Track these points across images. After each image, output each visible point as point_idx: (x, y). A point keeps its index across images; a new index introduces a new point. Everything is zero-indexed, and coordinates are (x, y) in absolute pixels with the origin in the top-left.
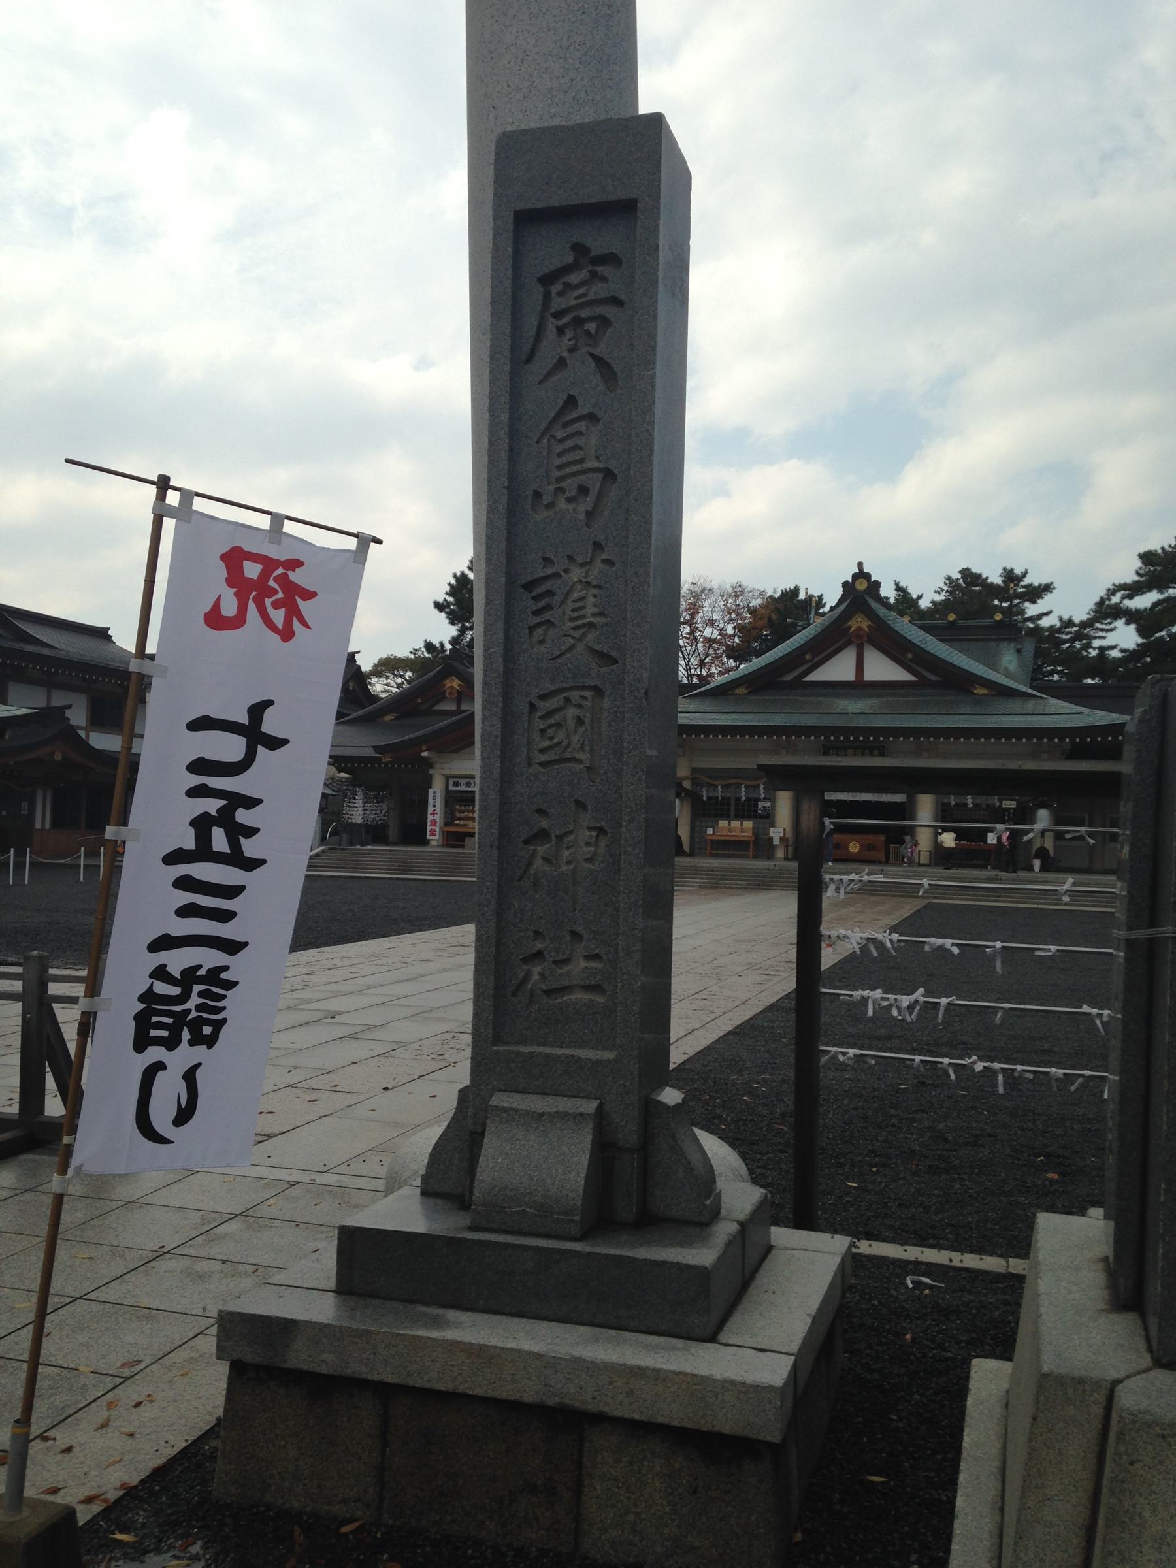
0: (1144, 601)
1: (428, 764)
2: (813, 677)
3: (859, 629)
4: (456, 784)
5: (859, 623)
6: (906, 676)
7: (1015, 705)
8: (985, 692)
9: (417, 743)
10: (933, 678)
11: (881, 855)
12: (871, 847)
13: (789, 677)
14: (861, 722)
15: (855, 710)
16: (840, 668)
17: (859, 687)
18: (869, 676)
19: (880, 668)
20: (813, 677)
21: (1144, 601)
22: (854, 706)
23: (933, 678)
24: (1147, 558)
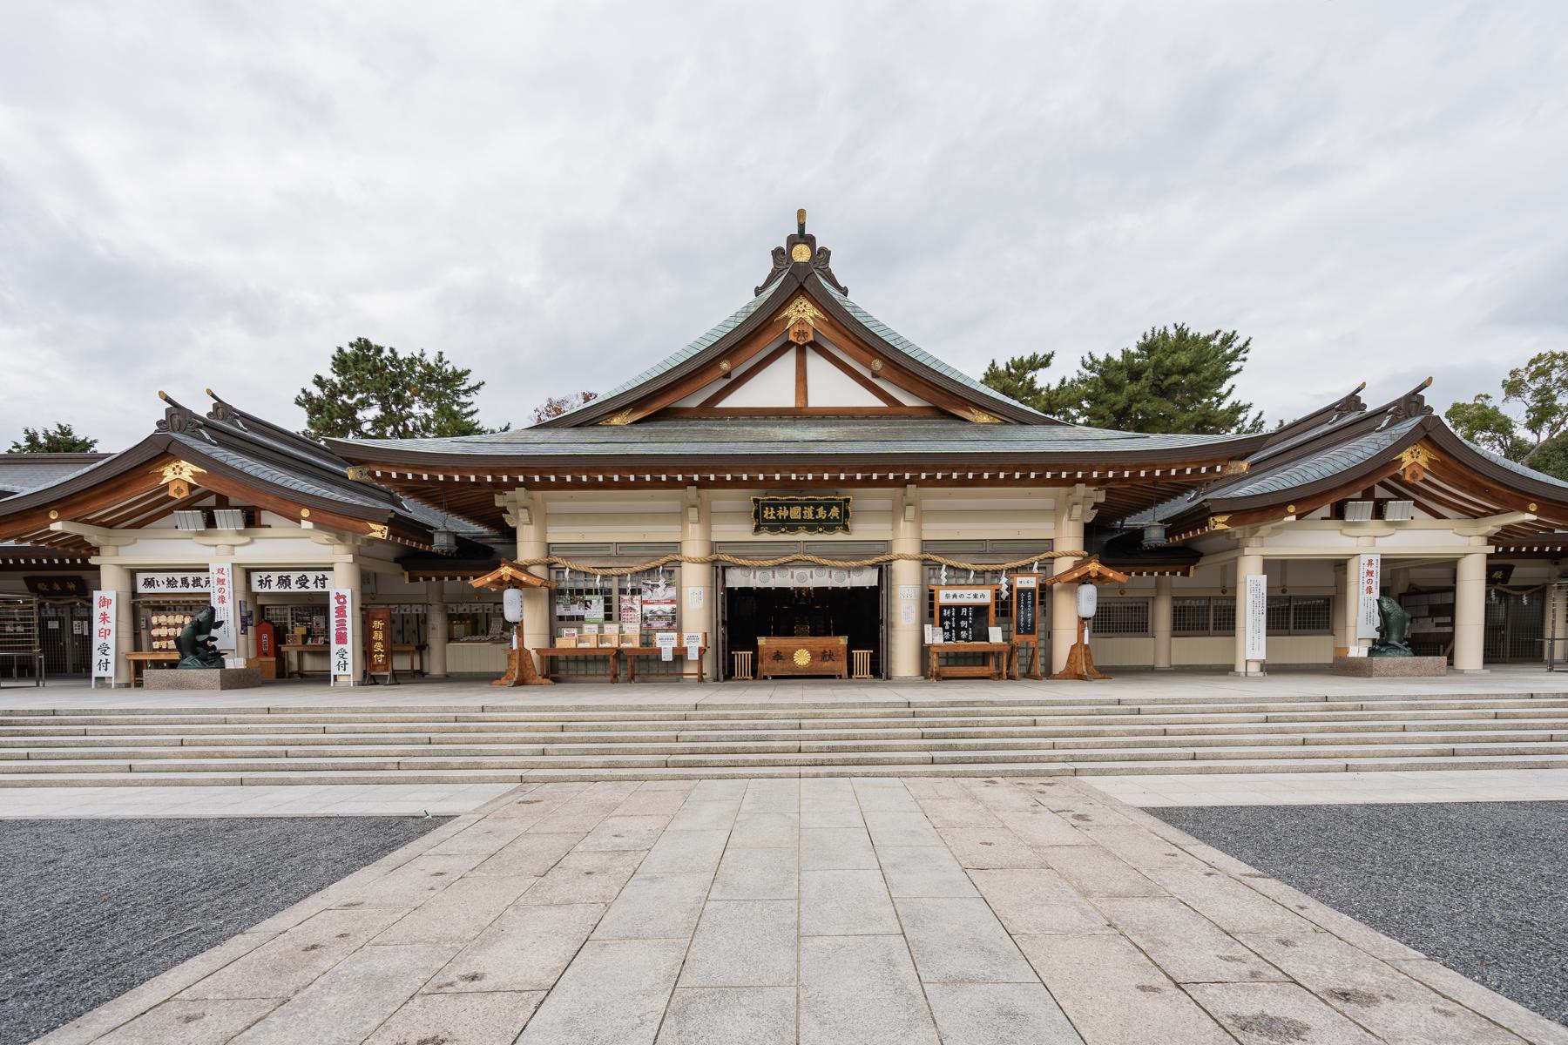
2: (728, 402)
3: (801, 322)
4: (149, 583)
5: (803, 312)
6: (871, 401)
8: (985, 419)
10: (908, 401)
11: (842, 667)
12: (826, 655)
13: (694, 402)
16: (772, 387)
17: (800, 414)
18: (816, 400)
19: (832, 387)
20: (728, 402)
23: (908, 401)
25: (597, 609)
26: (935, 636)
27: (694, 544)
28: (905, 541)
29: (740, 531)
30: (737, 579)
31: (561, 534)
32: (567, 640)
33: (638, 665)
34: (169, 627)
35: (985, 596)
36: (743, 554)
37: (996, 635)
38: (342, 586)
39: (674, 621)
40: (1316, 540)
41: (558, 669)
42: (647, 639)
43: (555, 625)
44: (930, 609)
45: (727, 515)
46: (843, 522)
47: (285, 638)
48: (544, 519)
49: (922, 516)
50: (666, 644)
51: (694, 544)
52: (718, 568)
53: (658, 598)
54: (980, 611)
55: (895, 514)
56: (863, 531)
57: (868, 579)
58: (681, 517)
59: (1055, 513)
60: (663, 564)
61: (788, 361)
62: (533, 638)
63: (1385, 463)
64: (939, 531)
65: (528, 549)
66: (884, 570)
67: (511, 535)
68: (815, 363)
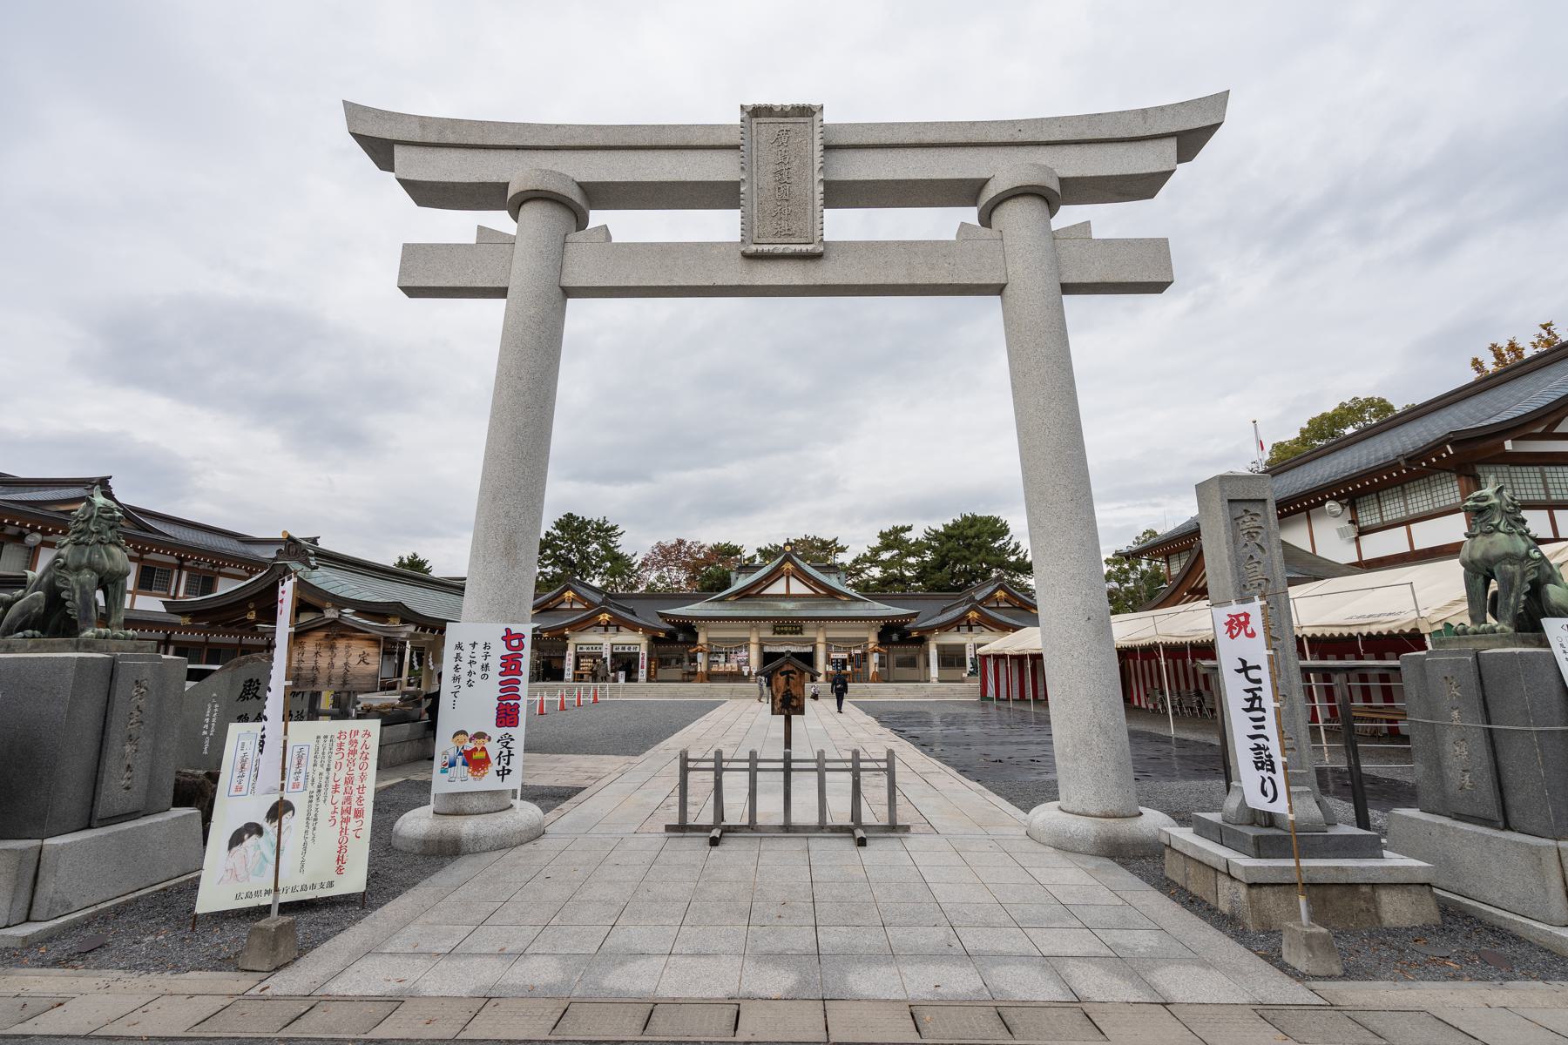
0: (885, 556)
1: (566, 638)
2: (765, 592)
7: (860, 605)
9: (563, 627)
14: (794, 614)
15: (789, 607)
16: (779, 588)
17: (788, 597)
18: (792, 592)
19: (797, 588)
20: (765, 592)
21: (885, 556)
22: (790, 605)
24: (882, 535)
25: (723, 659)
26: (830, 669)
27: (754, 639)
28: (821, 639)
29: (768, 634)
30: (767, 649)
31: (713, 634)
32: (715, 668)
33: (737, 677)
34: (586, 664)
35: (845, 656)
36: (770, 641)
37: (849, 668)
38: (643, 651)
39: (747, 663)
40: (953, 638)
41: (711, 677)
42: (740, 667)
43: (710, 664)
44: (829, 660)
45: (766, 629)
46: (801, 632)
47: (626, 664)
48: (709, 629)
49: (826, 629)
50: (745, 670)
51: (754, 639)
52: (761, 646)
53: (742, 655)
54: (844, 661)
55: (817, 629)
56: (807, 634)
57: (809, 649)
58: (750, 629)
59: (868, 629)
60: (745, 644)
61: (783, 580)
62: (702, 668)
63: (963, 617)
64: (831, 634)
65: (702, 639)
66: (814, 647)
67: (696, 635)
68: (792, 580)
